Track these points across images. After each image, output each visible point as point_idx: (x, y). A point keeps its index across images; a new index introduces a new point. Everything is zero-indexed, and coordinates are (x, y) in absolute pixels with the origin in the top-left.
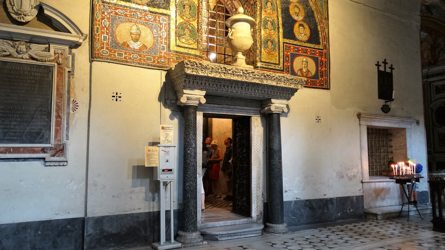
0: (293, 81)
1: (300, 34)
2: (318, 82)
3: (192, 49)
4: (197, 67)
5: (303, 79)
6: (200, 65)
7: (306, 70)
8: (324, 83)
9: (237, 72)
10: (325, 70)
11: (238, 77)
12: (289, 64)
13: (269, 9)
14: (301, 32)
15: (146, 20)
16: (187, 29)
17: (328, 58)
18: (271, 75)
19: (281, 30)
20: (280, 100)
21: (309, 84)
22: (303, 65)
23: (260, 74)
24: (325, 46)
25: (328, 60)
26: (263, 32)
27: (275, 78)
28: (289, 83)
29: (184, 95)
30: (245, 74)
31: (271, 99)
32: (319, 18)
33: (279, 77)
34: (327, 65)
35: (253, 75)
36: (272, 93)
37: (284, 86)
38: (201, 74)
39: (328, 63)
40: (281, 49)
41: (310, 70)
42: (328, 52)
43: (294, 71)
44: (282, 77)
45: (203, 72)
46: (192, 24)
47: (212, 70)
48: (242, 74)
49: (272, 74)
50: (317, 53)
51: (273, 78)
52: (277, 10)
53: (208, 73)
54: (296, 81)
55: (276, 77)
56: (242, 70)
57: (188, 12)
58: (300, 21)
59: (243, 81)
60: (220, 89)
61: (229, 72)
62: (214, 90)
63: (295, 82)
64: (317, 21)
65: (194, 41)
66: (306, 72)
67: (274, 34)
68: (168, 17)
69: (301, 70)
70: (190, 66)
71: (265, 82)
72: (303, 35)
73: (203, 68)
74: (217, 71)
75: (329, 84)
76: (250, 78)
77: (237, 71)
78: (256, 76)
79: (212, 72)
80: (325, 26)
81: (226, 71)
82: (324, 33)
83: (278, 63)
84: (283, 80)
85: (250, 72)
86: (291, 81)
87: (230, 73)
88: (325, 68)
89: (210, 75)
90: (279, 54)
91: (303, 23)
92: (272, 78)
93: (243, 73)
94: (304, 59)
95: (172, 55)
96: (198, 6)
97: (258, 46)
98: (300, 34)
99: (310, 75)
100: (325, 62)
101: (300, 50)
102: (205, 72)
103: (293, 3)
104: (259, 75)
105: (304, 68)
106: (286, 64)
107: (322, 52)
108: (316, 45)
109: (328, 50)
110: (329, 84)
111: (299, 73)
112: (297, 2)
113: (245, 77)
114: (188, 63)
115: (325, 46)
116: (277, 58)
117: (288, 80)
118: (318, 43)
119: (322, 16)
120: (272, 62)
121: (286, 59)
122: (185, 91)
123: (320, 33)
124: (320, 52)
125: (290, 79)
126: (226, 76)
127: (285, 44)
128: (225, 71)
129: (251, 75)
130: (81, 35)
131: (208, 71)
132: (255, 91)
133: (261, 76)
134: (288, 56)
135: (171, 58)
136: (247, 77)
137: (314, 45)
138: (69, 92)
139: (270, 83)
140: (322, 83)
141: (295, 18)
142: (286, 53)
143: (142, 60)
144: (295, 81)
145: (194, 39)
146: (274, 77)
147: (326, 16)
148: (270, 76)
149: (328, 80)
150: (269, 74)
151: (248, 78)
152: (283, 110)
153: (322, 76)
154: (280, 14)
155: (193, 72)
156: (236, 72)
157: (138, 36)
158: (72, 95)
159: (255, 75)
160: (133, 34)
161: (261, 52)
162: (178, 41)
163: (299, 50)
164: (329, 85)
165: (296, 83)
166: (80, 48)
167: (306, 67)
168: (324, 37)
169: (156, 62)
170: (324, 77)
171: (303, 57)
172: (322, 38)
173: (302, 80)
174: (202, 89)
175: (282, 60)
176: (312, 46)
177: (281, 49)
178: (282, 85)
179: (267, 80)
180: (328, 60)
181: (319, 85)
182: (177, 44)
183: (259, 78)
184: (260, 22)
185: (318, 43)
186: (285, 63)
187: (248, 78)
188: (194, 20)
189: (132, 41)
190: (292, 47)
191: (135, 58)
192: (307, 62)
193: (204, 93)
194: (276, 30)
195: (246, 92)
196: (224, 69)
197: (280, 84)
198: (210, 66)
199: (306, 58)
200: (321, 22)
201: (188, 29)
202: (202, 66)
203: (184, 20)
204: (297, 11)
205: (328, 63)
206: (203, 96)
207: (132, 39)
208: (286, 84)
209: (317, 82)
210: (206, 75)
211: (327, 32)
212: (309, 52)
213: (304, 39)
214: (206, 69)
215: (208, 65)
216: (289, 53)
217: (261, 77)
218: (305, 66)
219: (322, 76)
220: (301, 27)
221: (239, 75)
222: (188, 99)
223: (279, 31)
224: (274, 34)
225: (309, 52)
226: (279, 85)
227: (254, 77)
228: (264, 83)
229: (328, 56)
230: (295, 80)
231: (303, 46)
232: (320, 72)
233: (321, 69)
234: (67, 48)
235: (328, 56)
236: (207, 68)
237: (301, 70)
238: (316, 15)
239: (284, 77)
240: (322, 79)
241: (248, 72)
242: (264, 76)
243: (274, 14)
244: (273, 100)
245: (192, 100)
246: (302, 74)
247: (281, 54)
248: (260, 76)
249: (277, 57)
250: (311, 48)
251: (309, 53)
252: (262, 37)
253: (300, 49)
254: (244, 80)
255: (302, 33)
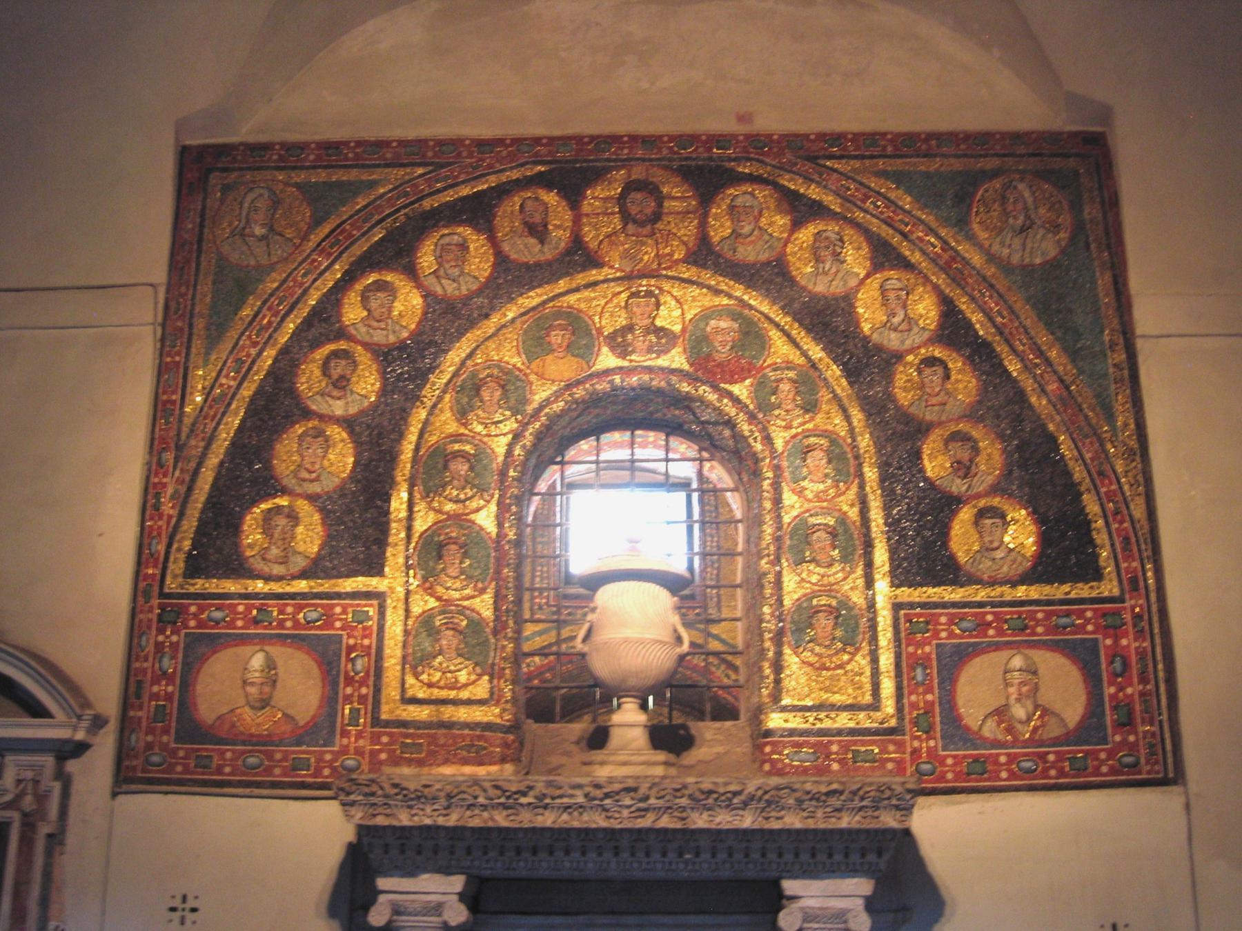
0: (843, 798)
1: (988, 550)
2: (1103, 756)
3: (469, 702)
4: (386, 796)
5: (896, 783)
6: (396, 791)
7: (1030, 708)
8: (1138, 759)
9: (561, 797)
10: (1142, 694)
11: (570, 814)
12: (929, 697)
13: (815, 478)
14: (991, 542)
15: (297, 624)
16: (450, 633)
17: (1156, 631)
18: (721, 790)
19: (881, 556)
20: (827, 882)
21: (1053, 772)
22: (1012, 690)
23: (666, 792)
24: (1134, 582)
25: (1158, 640)
26: (790, 582)
27: (742, 797)
28: (829, 810)
29: (382, 898)
30: (594, 799)
31: (781, 878)
32: (1092, 459)
33: (766, 792)
34: (1155, 667)
35: (633, 799)
36: (772, 856)
37: (798, 825)
38: (404, 819)
39: (1159, 657)
40: (885, 637)
41: (1057, 707)
42: (1154, 608)
43: (960, 726)
44: (778, 788)
45: (414, 812)
46: (473, 610)
47: (448, 800)
48: (581, 800)
49: (726, 784)
50: (1088, 621)
51: (735, 801)
52: (860, 475)
53: (436, 813)
54: (862, 799)
55: (746, 792)
56: (579, 786)
57: (456, 566)
58: (978, 496)
59: (594, 826)
60: (522, 864)
61: (524, 800)
62: (494, 866)
63: (857, 803)
64: (1078, 473)
65: (478, 670)
66: (1029, 719)
67: (845, 579)
68: (375, 602)
69: (1001, 713)
70: (360, 798)
71: (700, 821)
72: (999, 554)
73: (412, 799)
74: (471, 801)
75: (1169, 755)
76: (625, 813)
77: (549, 791)
78: (652, 801)
79: (448, 807)
80: (1126, 487)
81: (508, 798)
82: (1121, 522)
83: (868, 698)
84: (791, 801)
85: (617, 787)
86: (835, 802)
87: (530, 804)
88: (1143, 680)
89: (441, 821)
90: (875, 661)
91: (996, 501)
92: (730, 800)
93: (586, 796)
94: (1017, 662)
95: (385, 739)
96: (498, 535)
97: (767, 644)
98: (988, 550)
99: (1054, 731)
100: (1141, 654)
101: (989, 624)
102: (421, 813)
103: (940, 424)
104: (662, 797)
105: (1018, 700)
106: (913, 698)
107: (1117, 613)
108: (1080, 585)
109: (1153, 597)
110: (1169, 755)
111: (990, 730)
112: (965, 416)
113: (600, 809)
114: (346, 785)
115: (1134, 582)
116: (866, 679)
117: (818, 800)
118: (1098, 575)
119: (1109, 446)
120: (837, 698)
121: (914, 678)
122: (382, 883)
123: (1100, 523)
124: (1104, 615)
125: (828, 794)
126: (512, 818)
127: (902, 612)
128: (502, 800)
129: (628, 802)
130: (74, 720)
131: (436, 807)
132: (681, 855)
133: (676, 797)
134: (925, 662)
135: (380, 751)
136: (607, 810)
137: (1066, 588)
138: (45, 902)
139: (724, 820)
140: (1131, 755)
141: (955, 490)
142: (911, 649)
143: (277, 771)
144: (857, 798)
145: (476, 664)
146: (736, 794)
147: (1133, 443)
148: (715, 796)
149: (1167, 735)
150: (710, 787)
151: (617, 815)
152: (845, 922)
153: (1127, 723)
154: (875, 485)
155: (374, 816)
156: (553, 798)
157: (267, 689)
158: (54, 909)
159: (647, 798)
160: (252, 684)
161: (778, 667)
162: (410, 680)
163: (983, 626)
164: (1170, 760)
165: (864, 803)
166: (88, 753)
167: (1028, 697)
168: (1126, 540)
169: (326, 772)
170: (1141, 729)
171: (1005, 654)
172: (1112, 545)
173: (889, 788)
174: (447, 871)
175: (888, 686)
176: (1059, 591)
177: (885, 637)
178: (794, 821)
179: (709, 809)
180: (1158, 640)
181: (1112, 768)
182: (410, 693)
183: (669, 808)
184: (778, 540)
185: (1098, 575)
186: (910, 694)
187: (617, 815)
188: (483, 591)
189: (247, 709)
190: (943, 619)
191: (254, 769)
192: (1035, 673)
193: (457, 883)
194: (856, 557)
195: (644, 866)
196: (499, 792)
197: (778, 818)
198: (438, 786)
199: (1027, 652)
200: (1100, 473)
201: (453, 629)
202: (405, 792)
203: (439, 599)
204: (965, 455)
205: (1159, 657)
206: (455, 898)
207: (248, 703)
208: (812, 817)
209: (1097, 759)
210: (428, 821)
211: (1138, 511)
212: (1038, 622)
213: (1005, 569)
214: (423, 800)
215: (426, 786)
216: (927, 649)
217: (677, 801)
218: (1025, 689)
219: (1127, 723)
220: (988, 522)
221: (569, 807)
222: (397, 911)
223: (869, 565)
224: (845, 579)
225: (1038, 622)
226: (776, 825)
227: (642, 805)
228: (694, 827)
229: (1156, 625)
230: (854, 793)
231: (1003, 604)
232: (1115, 708)
233: (1121, 689)
234: (49, 761)
235: (1156, 625)
236: (426, 797)
237: (1001, 713)
238: (1066, 449)
239: (794, 791)
240: (1124, 741)
241: (605, 790)
242: (691, 797)
243: (844, 493)
244: (790, 886)
245: (410, 914)
246: (1010, 730)
247: (886, 660)
248: (667, 798)
249: (861, 674)
250: (1049, 603)
251: (1040, 630)
252: (787, 602)
253: (989, 618)
254: (597, 820)
255: (996, 544)
